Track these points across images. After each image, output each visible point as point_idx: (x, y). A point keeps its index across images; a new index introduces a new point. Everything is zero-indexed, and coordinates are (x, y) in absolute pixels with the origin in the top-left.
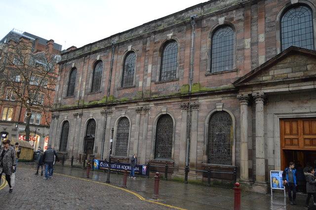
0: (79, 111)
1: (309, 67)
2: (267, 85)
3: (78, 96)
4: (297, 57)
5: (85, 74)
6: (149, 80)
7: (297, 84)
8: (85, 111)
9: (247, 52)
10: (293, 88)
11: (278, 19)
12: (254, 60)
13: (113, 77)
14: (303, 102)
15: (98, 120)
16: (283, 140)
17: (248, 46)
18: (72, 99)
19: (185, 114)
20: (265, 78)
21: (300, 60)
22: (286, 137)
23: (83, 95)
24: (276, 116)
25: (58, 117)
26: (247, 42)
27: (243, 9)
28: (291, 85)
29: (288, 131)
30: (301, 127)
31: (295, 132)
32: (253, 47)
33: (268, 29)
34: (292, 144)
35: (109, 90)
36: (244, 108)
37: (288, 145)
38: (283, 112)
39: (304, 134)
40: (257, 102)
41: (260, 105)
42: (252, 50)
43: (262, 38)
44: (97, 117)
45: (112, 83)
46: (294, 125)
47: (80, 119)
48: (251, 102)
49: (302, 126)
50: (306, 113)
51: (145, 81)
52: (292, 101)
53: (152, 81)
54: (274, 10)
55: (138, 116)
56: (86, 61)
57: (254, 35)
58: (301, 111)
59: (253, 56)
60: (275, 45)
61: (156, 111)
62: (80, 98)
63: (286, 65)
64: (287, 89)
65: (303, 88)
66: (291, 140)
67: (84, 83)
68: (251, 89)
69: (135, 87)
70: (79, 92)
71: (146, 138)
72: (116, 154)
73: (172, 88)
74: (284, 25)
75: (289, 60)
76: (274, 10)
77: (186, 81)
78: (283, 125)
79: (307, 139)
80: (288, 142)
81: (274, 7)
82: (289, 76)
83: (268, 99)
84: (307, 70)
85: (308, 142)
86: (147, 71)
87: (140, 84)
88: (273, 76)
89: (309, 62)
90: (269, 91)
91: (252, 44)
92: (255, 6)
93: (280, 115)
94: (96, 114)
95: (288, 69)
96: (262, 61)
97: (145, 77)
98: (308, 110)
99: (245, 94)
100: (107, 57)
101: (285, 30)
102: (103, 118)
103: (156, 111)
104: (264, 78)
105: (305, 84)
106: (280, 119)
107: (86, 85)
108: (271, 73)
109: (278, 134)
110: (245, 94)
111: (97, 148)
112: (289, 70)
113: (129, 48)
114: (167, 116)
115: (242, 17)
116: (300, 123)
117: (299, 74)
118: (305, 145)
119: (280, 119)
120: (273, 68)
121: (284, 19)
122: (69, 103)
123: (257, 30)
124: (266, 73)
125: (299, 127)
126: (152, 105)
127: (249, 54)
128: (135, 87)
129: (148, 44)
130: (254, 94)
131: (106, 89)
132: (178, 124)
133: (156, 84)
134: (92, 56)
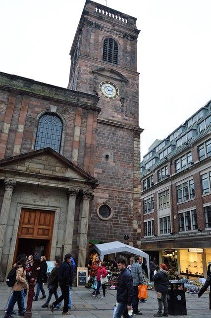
1: (57, 168)
2: (20, 174)
4: (50, 158)
7: (45, 181)
9: (4, 137)
10: (42, 183)
11: (38, 118)
12: (9, 146)
14: (44, 196)
16: (21, 229)
17: (6, 131)
21: (52, 161)
22: (24, 226)
24: (19, 205)
27: (8, 93)
28: (41, 180)
29: (26, 220)
30: (37, 218)
31: (32, 222)
32: (11, 134)
33: (28, 123)
34: (27, 233)
37: (24, 234)
38: (27, 202)
39: (39, 225)
40: (6, 189)
42: (9, 135)
43: (21, 129)
46: (33, 215)
49: (38, 218)
50: (45, 206)
52: (36, 194)
54: (37, 109)
57: (14, 122)
58: (41, 204)
59: (10, 144)
60: (32, 139)
63: (41, 161)
64: (37, 183)
65: (50, 185)
66: (28, 229)
68: (4, 174)
74: (41, 125)
75: (44, 158)
76: (37, 109)
78: (23, 214)
79: (41, 229)
80: (25, 231)
81: (37, 106)
82: (42, 172)
83: (19, 188)
84: (55, 171)
85: (41, 232)
88: (28, 168)
89: (58, 164)
91: (11, 131)
92: (20, 96)
93: (23, 205)
95: (42, 165)
96: (17, 150)
98: (47, 205)
101: (41, 130)
104: (19, 168)
105: (51, 181)
106: (22, 208)
108: (27, 164)
109: (17, 223)
112: (42, 167)
115: (5, 100)
116: (38, 214)
117: (50, 173)
118: (38, 234)
119: (22, 208)
120: (29, 160)
121: (42, 121)
123: (18, 120)
124: (22, 163)
125: (36, 219)
127: (6, 139)
130: (7, 180)
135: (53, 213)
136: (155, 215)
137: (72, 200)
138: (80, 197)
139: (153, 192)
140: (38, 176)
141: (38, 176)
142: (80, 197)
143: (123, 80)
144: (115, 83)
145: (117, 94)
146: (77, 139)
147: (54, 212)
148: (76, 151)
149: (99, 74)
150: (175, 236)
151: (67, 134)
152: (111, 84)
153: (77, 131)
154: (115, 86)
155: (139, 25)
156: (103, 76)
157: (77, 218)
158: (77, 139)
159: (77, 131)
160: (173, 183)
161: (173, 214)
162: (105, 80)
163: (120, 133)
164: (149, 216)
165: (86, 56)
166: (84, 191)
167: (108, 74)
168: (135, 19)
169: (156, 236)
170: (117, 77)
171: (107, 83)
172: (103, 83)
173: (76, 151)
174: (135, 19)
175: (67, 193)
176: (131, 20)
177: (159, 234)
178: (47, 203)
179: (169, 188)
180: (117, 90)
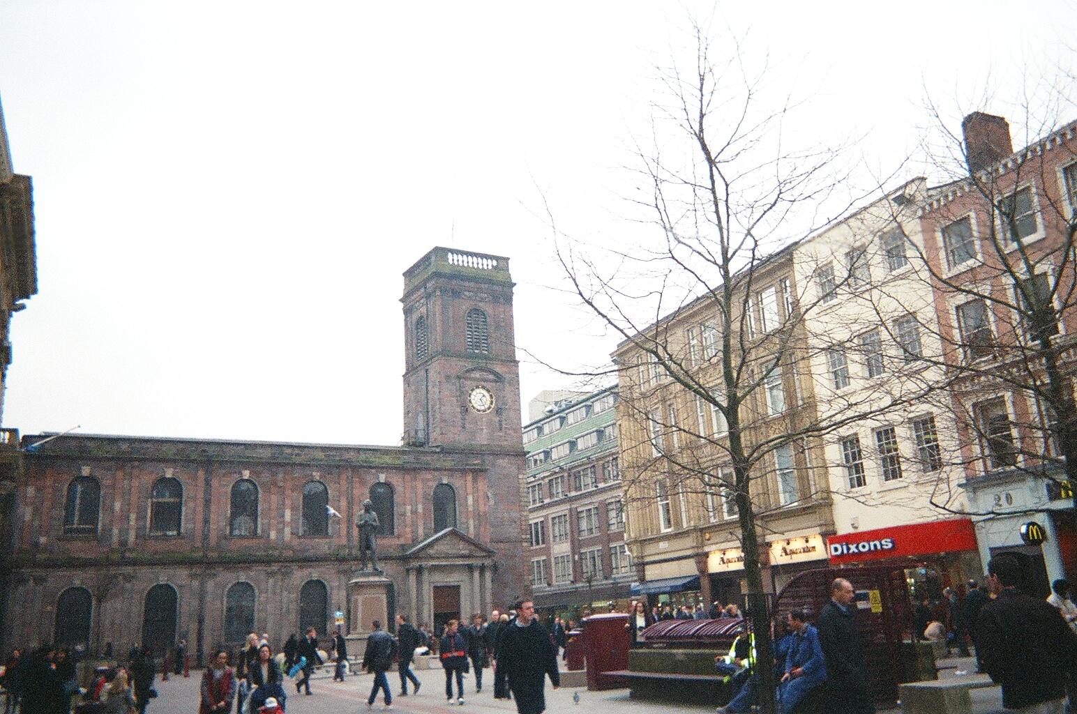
0: (129, 570)
1: (461, 546)
2: (432, 558)
3: (115, 539)
5: (134, 499)
6: (287, 530)
8: (144, 571)
9: (408, 521)
13: (213, 517)
15: (180, 587)
17: (409, 514)
18: (94, 543)
19: (343, 579)
20: (431, 552)
23: (132, 537)
25: (39, 581)
26: (409, 508)
35: (206, 537)
36: (412, 578)
41: (426, 575)
43: (420, 510)
44: (179, 582)
45: (213, 527)
47: (128, 585)
48: (420, 571)
51: (280, 532)
53: (292, 534)
54: (431, 484)
55: (271, 581)
56: (128, 470)
59: (415, 525)
61: (299, 576)
62: (123, 543)
65: (457, 563)
67: (133, 516)
69: (261, 537)
70: (115, 531)
71: (288, 611)
72: (226, 640)
73: (322, 545)
76: (431, 484)
77: (344, 541)
86: (283, 516)
87: (273, 535)
90: (434, 563)
91: (412, 512)
94: (179, 578)
97: (281, 526)
99: (415, 564)
100: (195, 478)
102: (196, 583)
103: (299, 576)
107: (137, 520)
108: (436, 547)
110: (415, 564)
111: (185, 636)
112: (448, 547)
113: (246, 474)
114: (320, 584)
117: (455, 551)
119: (436, 587)
122: (79, 548)
126: (294, 566)
128: (261, 537)
129: (280, 476)
131: (199, 533)
132: (335, 592)
133: (299, 537)
134: (150, 466)
135: (458, 587)
136: (547, 551)
137: (476, 574)
138: (482, 569)
139: (544, 513)
140: (447, 557)
141: (447, 557)
142: (482, 569)
143: (499, 378)
144: (488, 385)
145: (492, 403)
146: (470, 509)
147: (458, 587)
148: (471, 522)
149: (466, 379)
150: (577, 585)
151: (460, 505)
152: (483, 388)
153: (470, 500)
154: (488, 391)
155: (515, 273)
156: (471, 379)
157: (482, 586)
158: (470, 509)
159: (470, 500)
160: (573, 506)
161: (574, 553)
162: (474, 384)
163: (502, 462)
164: (537, 553)
165: (445, 353)
166: (486, 564)
167: (477, 375)
168: (508, 259)
169: (549, 585)
170: (491, 377)
171: (477, 387)
172: (472, 390)
173: (471, 522)
174: (508, 259)
175: (470, 568)
176: (502, 264)
177: (554, 583)
178: (452, 579)
179: (567, 512)
180: (491, 396)
